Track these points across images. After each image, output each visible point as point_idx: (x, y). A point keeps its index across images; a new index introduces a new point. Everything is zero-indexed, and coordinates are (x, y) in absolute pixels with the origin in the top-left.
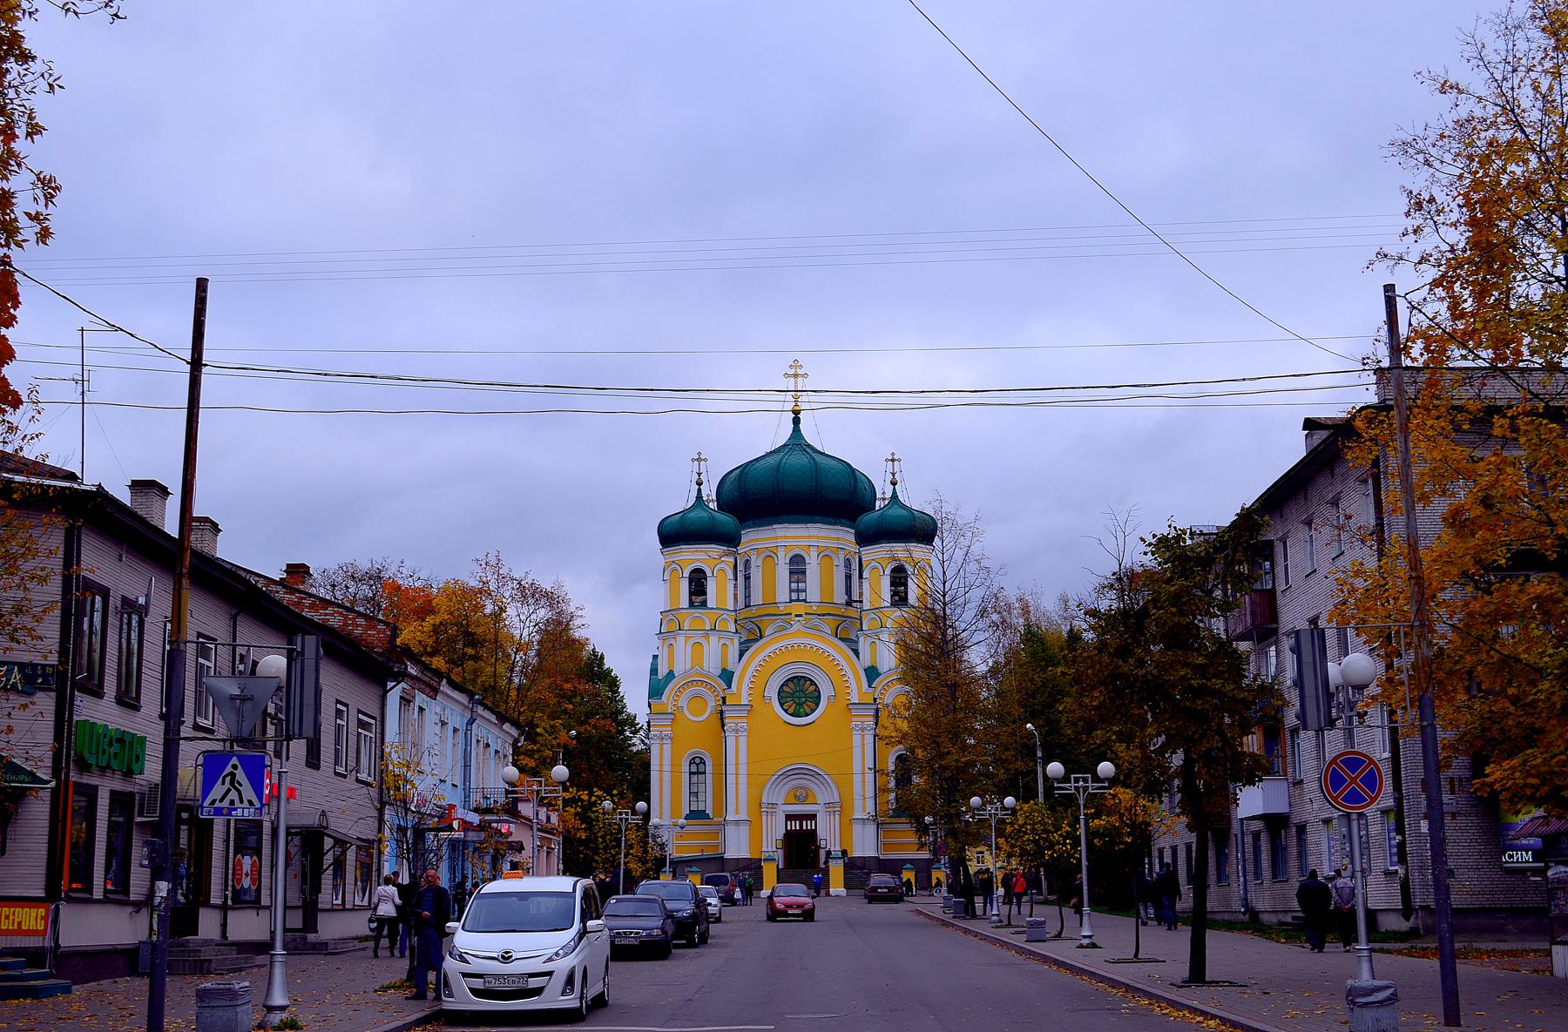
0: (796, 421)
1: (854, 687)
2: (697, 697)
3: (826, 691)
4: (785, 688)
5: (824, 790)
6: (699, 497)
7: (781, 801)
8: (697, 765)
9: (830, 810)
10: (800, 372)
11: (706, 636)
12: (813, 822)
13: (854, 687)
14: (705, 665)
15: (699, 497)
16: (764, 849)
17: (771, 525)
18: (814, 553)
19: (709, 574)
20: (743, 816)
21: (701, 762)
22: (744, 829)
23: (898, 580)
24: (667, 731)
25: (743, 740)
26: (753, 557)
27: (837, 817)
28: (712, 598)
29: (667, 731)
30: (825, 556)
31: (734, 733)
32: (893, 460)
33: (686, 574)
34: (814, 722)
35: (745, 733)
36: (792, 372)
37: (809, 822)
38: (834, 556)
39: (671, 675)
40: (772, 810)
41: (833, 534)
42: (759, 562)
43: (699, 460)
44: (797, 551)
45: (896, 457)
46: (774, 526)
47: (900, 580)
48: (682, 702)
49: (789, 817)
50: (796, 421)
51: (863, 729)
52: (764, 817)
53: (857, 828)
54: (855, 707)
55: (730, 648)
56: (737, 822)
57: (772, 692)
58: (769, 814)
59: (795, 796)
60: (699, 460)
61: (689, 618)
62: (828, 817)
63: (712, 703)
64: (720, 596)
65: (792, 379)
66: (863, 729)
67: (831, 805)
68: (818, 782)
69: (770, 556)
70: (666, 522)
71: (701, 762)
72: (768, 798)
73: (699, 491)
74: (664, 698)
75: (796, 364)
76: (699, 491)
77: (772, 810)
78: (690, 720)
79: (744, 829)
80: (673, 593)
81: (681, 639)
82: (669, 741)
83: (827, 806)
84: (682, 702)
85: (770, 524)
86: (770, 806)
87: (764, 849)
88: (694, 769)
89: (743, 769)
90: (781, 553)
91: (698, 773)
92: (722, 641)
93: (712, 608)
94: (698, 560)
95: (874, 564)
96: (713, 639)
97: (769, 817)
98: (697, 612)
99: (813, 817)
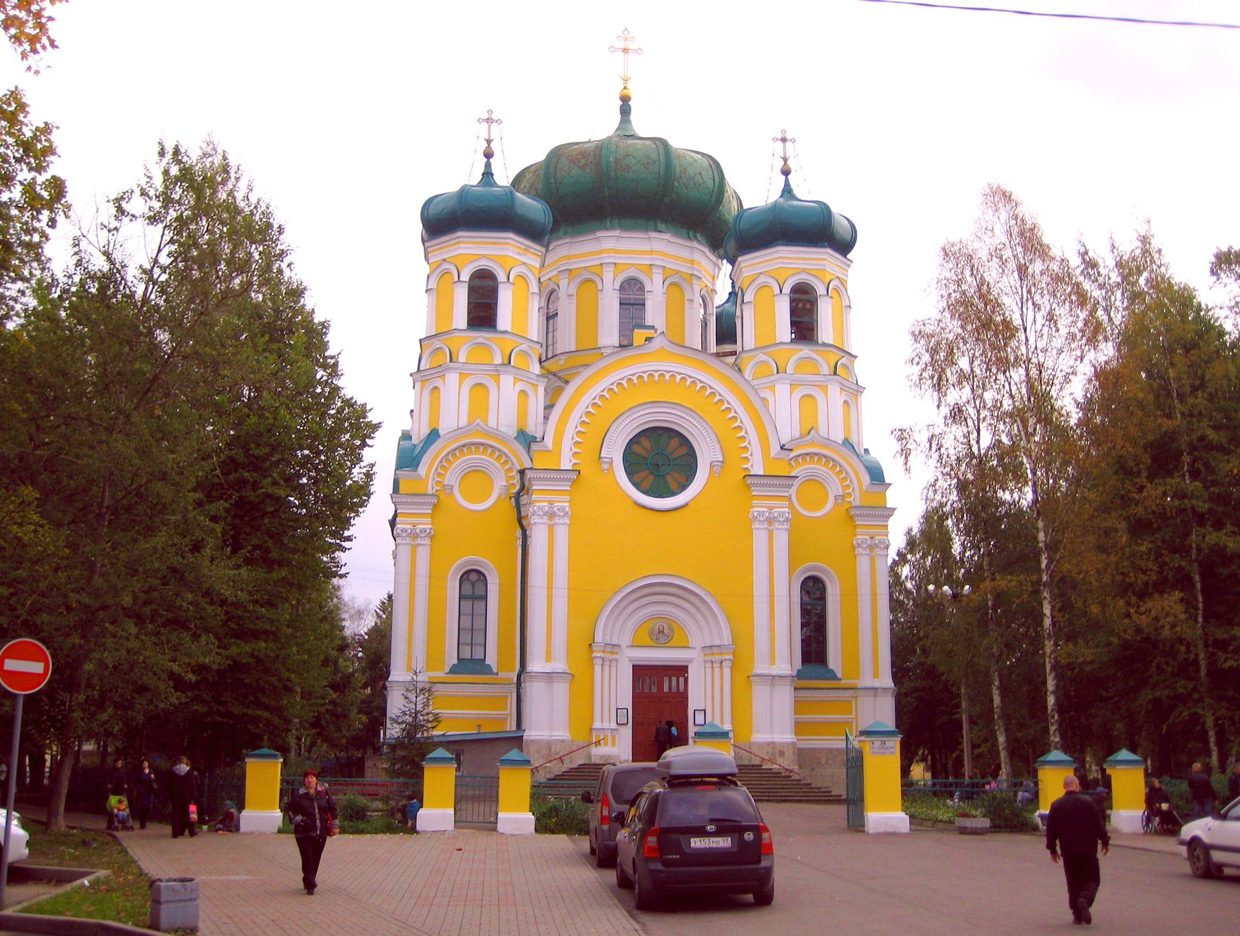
0: (625, 110)
1: (756, 448)
2: (475, 470)
3: (706, 454)
4: (637, 448)
5: (703, 624)
6: (488, 174)
7: (625, 640)
8: (473, 584)
9: (717, 658)
10: (630, 45)
11: (496, 372)
12: (682, 680)
13: (756, 448)
14: (492, 422)
15: (488, 174)
16: (597, 725)
17: (595, 232)
18: (658, 278)
19: (501, 277)
20: (559, 665)
21: (479, 580)
22: (561, 690)
23: (800, 305)
24: (425, 525)
25: (562, 534)
26: (563, 283)
27: (727, 671)
28: (505, 318)
29: (425, 525)
30: (677, 284)
31: (545, 519)
32: (784, 140)
33: (465, 277)
34: (687, 504)
35: (566, 520)
36: (621, 45)
37: (674, 679)
38: (686, 286)
39: (434, 435)
40: (611, 657)
41: (685, 253)
42: (573, 290)
43: (489, 121)
44: (632, 273)
45: (788, 137)
46: (599, 234)
47: (804, 305)
48: (452, 477)
49: (640, 671)
50: (625, 110)
51: (770, 521)
52: (598, 669)
53: (760, 693)
54: (755, 481)
55: (532, 399)
56: (550, 677)
57: (615, 451)
58: (606, 663)
59: (651, 634)
60: (489, 121)
61: (468, 344)
62: (709, 671)
63: (502, 482)
64: (520, 314)
65: (621, 55)
66: (770, 521)
67: (715, 650)
68: (693, 610)
69: (588, 282)
70: (432, 205)
71: (479, 580)
72: (604, 635)
73: (488, 165)
74: (422, 470)
75: (626, 35)
76: (488, 165)
77: (611, 657)
78: (465, 508)
79: (561, 690)
80: (441, 308)
81: (452, 378)
82: (427, 541)
83: (708, 651)
84: (452, 477)
85: (593, 231)
86: (609, 649)
87: (597, 725)
88: (468, 589)
89: (561, 580)
90: (608, 274)
91: (473, 598)
92: (520, 386)
93: (506, 332)
94: (484, 256)
95: (762, 279)
96: (507, 380)
97: (606, 669)
98: (482, 336)
99: (681, 671)
